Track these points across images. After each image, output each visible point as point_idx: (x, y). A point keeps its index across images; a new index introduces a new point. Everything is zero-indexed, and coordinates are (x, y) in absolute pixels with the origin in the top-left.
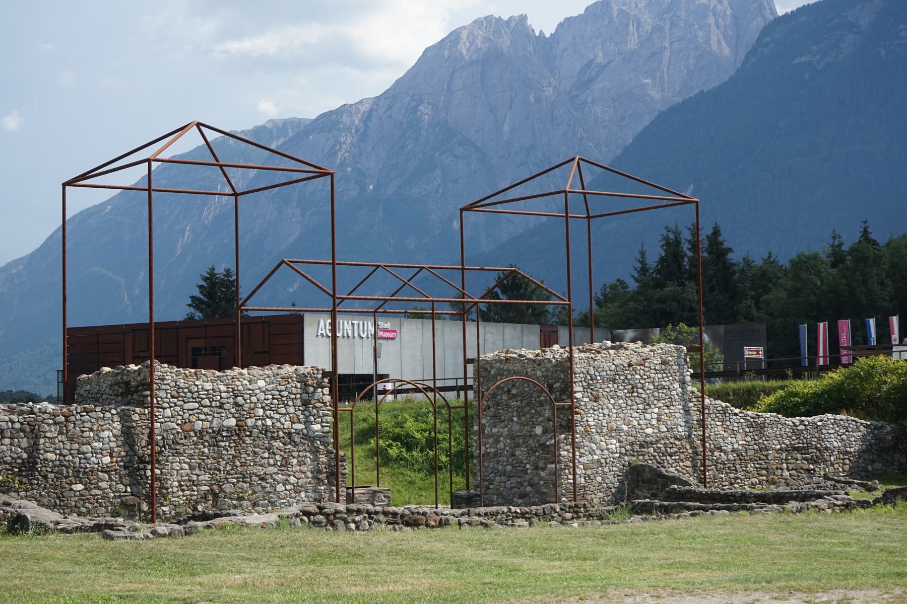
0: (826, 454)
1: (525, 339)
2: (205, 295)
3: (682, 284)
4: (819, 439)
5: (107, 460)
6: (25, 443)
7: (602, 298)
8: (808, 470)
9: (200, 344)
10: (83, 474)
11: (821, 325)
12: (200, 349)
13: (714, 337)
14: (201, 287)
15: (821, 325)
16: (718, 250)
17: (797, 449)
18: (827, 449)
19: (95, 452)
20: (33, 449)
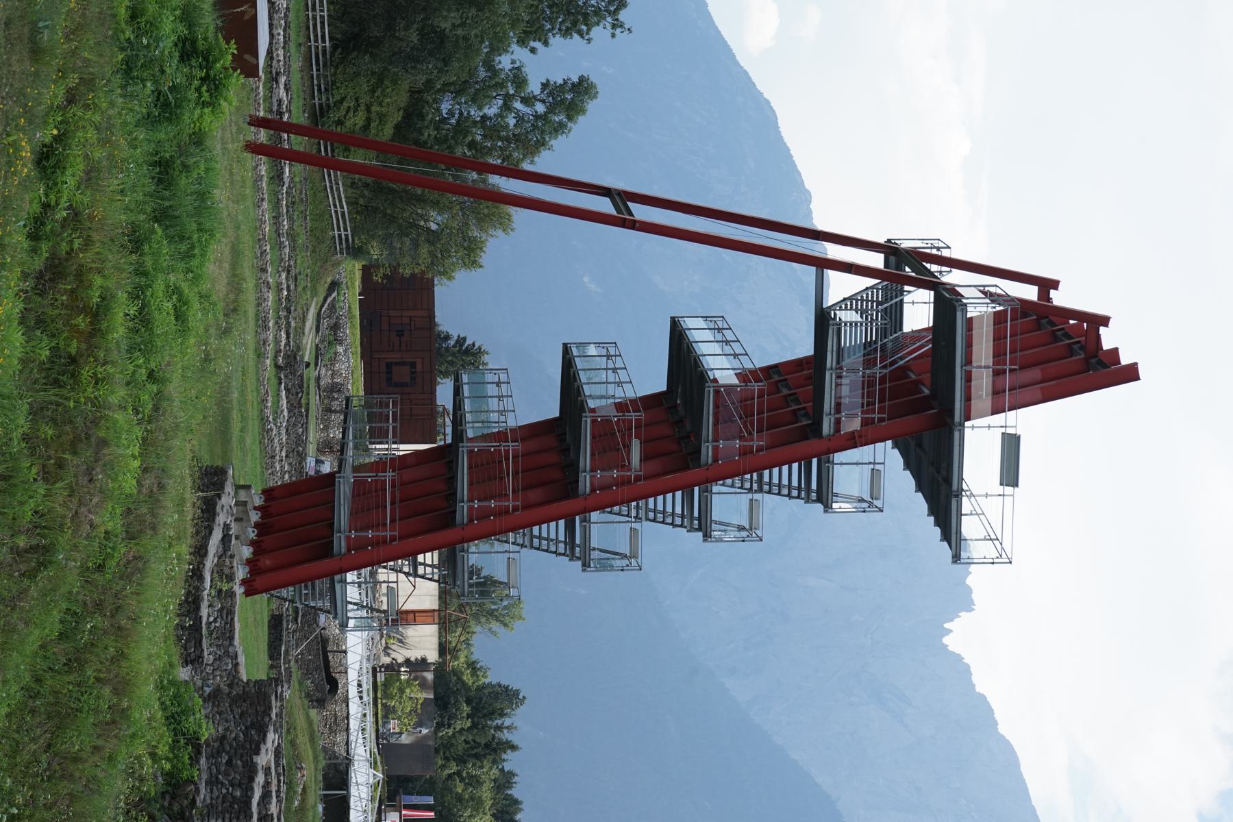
0: (333, 734)
1: (428, 598)
2: (467, 348)
3: (468, 716)
4: (340, 731)
5: (332, 436)
6: (338, 409)
7: (478, 666)
8: (326, 725)
9: (419, 368)
10: (326, 428)
11: (433, 814)
12: (415, 367)
13: (425, 737)
14: (474, 345)
15: (433, 814)
16: (500, 749)
17: (336, 719)
18: (336, 734)
19: (334, 432)
20: (335, 411)
